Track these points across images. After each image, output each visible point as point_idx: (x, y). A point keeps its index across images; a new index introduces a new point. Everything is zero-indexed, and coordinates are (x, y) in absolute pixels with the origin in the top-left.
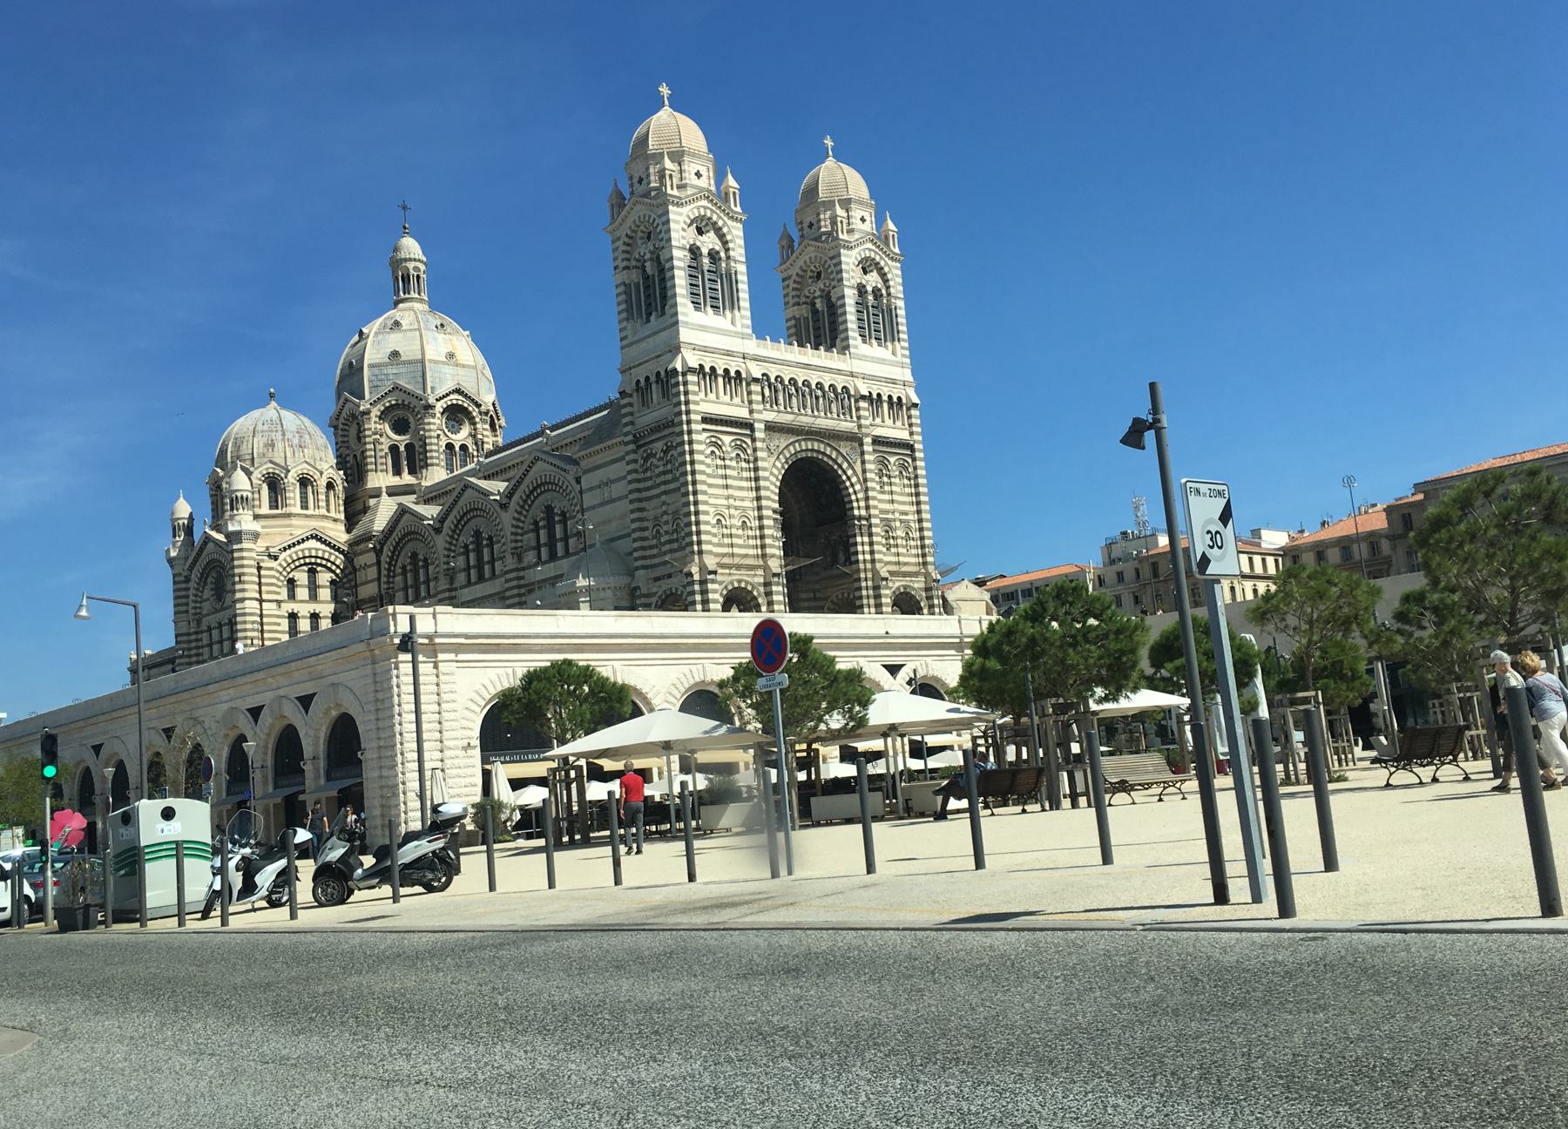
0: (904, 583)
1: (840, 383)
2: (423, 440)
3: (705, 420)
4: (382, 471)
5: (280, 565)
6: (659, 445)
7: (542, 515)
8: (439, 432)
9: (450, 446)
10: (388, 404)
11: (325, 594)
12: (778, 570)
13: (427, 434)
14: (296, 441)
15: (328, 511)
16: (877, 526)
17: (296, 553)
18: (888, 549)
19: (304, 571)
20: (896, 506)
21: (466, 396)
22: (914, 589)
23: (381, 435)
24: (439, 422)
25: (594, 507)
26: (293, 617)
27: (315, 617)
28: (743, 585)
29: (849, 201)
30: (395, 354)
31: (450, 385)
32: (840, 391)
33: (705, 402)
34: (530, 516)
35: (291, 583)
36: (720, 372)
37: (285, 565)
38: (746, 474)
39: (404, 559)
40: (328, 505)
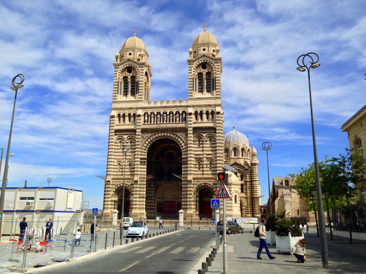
3: (116, 131)
22: (209, 184)
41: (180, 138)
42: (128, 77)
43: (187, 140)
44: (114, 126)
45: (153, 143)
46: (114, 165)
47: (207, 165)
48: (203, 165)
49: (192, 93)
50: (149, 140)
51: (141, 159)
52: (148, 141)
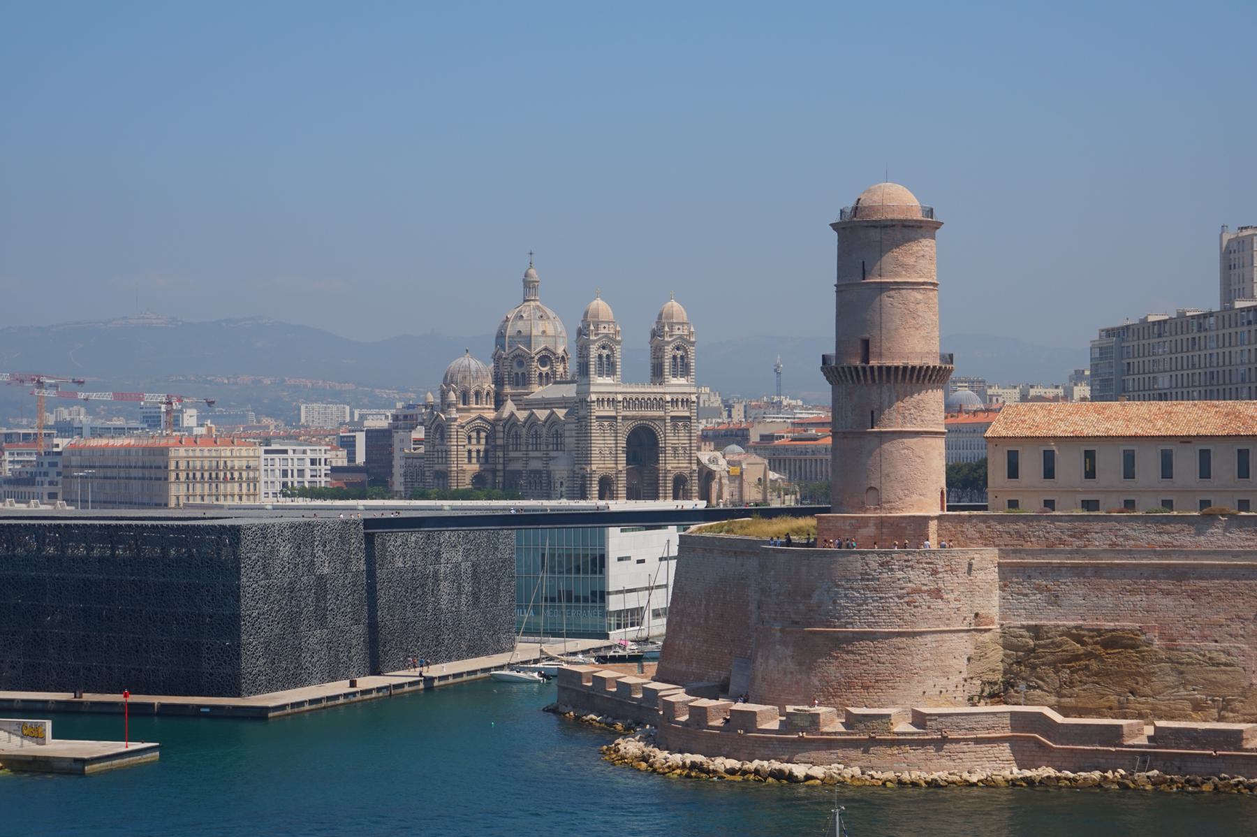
1: (658, 397)
2: (529, 372)
3: (598, 417)
9: (541, 374)
11: (483, 441)
14: (475, 375)
21: (550, 351)
26: (470, 452)
27: (478, 451)
30: (520, 332)
33: (598, 411)
35: (470, 438)
39: (513, 432)
41: (658, 427)
43: (665, 430)
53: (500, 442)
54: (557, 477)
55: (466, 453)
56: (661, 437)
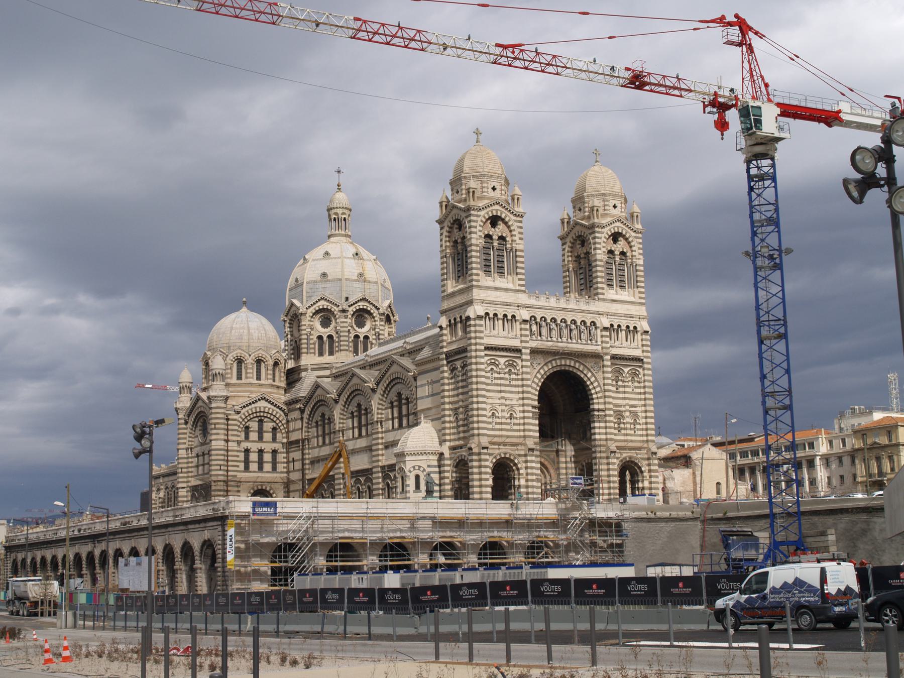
0: (629, 454)
1: (589, 319)
3: (487, 348)
4: (311, 353)
5: (241, 417)
6: (458, 364)
7: (395, 398)
8: (349, 328)
9: (357, 337)
10: (317, 309)
12: (534, 447)
13: (342, 329)
15: (274, 381)
16: (610, 415)
17: (251, 409)
18: (619, 431)
19: (255, 421)
20: (627, 401)
23: (313, 327)
24: (350, 321)
25: (422, 398)
26: (247, 451)
27: (261, 452)
28: (507, 456)
29: (604, 194)
30: (324, 275)
31: (359, 296)
32: (588, 324)
34: (388, 398)
36: (500, 316)
37: (244, 417)
38: (514, 383)
39: (317, 417)
40: (274, 377)
42: (494, 237)
44: (481, 338)
45: (548, 377)
46: (485, 416)
47: (631, 423)
48: (624, 423)
49: (603, 288)
50: (542, 372)
51: (534, 407)
52: (540, 374)
53: (295, 436)
54: (408, 466)
55: (243, 454)
56: (595, 391)
